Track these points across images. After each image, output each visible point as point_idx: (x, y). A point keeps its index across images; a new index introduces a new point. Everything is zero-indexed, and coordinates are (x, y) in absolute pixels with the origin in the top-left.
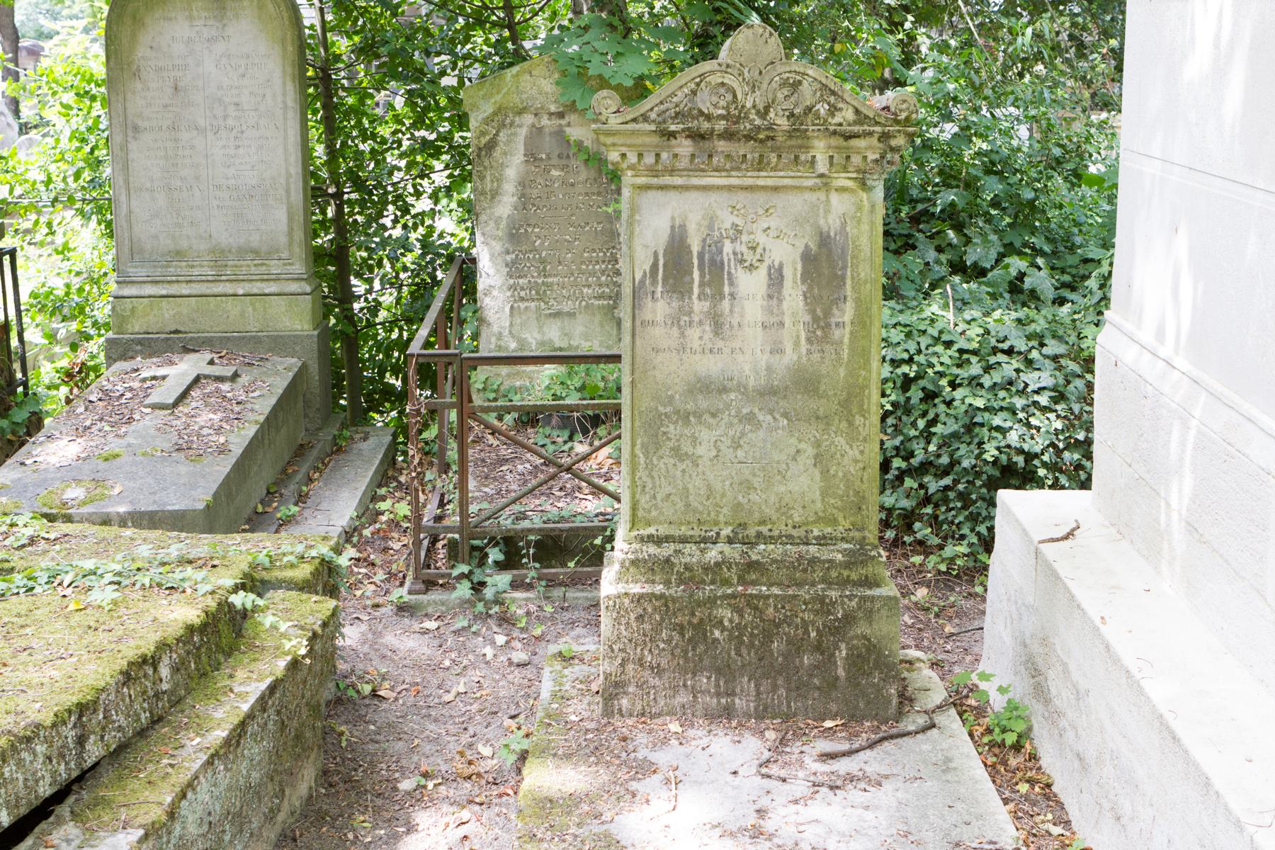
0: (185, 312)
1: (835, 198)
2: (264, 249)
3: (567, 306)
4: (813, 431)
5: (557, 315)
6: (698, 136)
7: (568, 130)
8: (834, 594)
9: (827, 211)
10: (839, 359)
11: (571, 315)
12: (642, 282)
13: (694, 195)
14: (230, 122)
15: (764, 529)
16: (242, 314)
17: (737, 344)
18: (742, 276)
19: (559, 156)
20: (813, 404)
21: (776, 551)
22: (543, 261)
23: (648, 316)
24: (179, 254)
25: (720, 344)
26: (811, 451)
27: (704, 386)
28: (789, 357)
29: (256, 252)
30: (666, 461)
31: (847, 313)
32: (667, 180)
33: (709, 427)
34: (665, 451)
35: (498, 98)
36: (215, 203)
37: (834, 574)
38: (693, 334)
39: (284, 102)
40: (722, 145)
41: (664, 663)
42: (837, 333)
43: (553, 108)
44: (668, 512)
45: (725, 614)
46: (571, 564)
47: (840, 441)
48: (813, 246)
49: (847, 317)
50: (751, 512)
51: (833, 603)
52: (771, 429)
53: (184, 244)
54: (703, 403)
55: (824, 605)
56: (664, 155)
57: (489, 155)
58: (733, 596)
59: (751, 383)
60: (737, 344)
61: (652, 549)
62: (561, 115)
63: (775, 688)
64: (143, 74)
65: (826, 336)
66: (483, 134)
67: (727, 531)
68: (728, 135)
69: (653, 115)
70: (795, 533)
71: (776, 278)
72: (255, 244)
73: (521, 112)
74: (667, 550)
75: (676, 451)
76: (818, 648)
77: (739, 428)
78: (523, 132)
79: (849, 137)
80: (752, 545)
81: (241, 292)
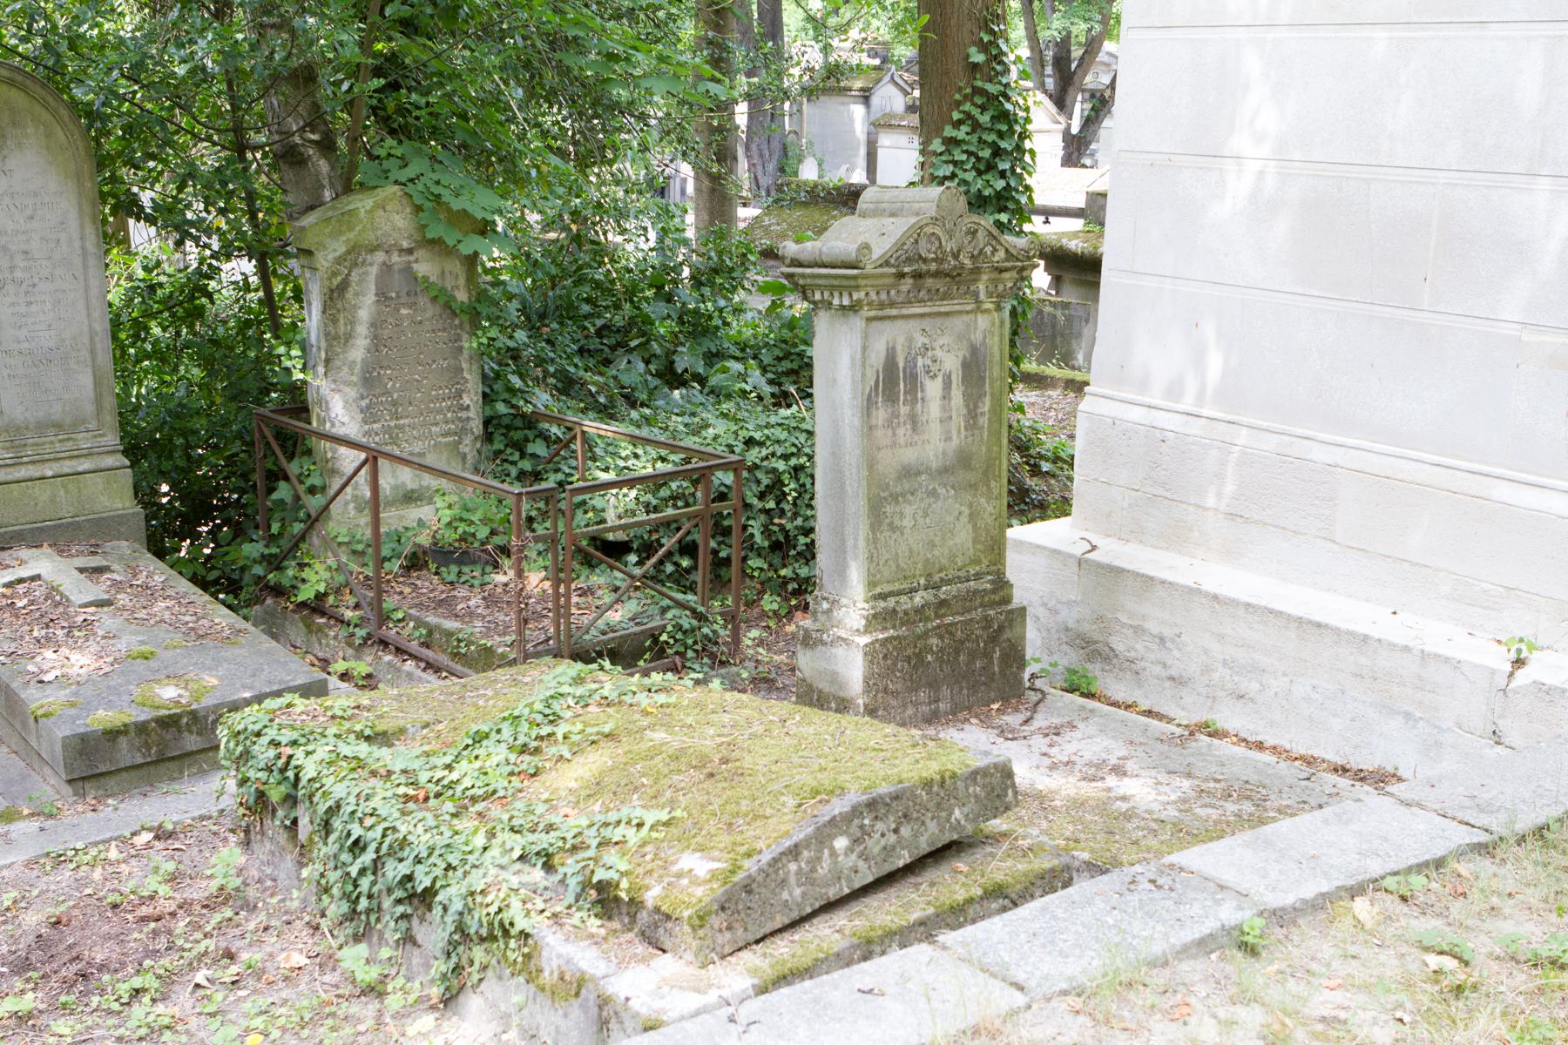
1: (980, 317)
4: (968, 496)
8: (992, 612)
13: (900, 322)
17: (926, 437)
23: (873, 422)
26: (967, 511)
28: (955, 441)
34: (884, 527)
38: (901, 431)
45: (934, 641)
52: (946, 499)
55: (987, 621)
58: (938, 627)
60: (926, 437)
61: (882, 604)
68: (937, 274)
79: (1001, 271)
80: (937, 587)
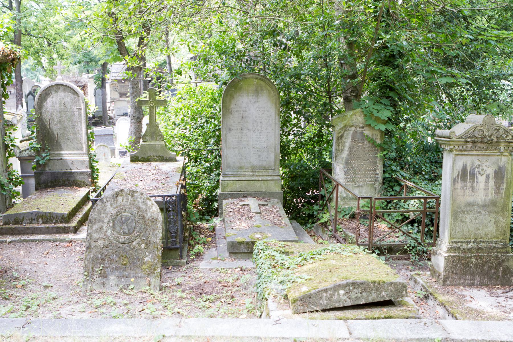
0: (243, 185)
1: (503, 158)
2: (267, 166)
3: (361, 184)
4: (494, 215)
5: (358, 186)
6: (474, 142)
7: (364, 132)
8: (500, 255)
9: (501, 161)
10: (502, 198)
11: (362, 186)
12: (455, 178)
13: (469, 157)
14: (259, 128)
15: (482, 240)
16: (261, 186)
17: (477, 194)
18: (480, 177)
19: (361, 140)
20: (495, 209)
21: (485, 245)
22: (355, 171)
23: (456, 187)
24: (241, 168)
25: (473, 194)
26: (494, 220)
27: (469, 204)
28: (490, 197)
29: (265, 167)
30: (458, 223)
31: (504, 186)
32: (464, 153)
33: (470, 215)
34: (459, 220)
35: (345, 122)
36: (253, 152)
37: (499, 250)
38: (467, 191)
39: (275, 122)
40: (479, 144)
41: (458, 272)
42: (501, 191)
43: (361, 125)
44: (458, 235)
45: (474, 260)
46: (397, 254)
47: (501, 218)
48: (497, 170)
49: (504, 187)
50: (478, 236)
51: (499, 257)
52: (484, 215)
53: (243, 165)
54: (468, 209)
55: (497, 258)
56: (464, 147)
57: (341, 139)
58: (476, 256)
59: (480, 203)
60: (477, 194)
61: (455, 245)
62: (363, 127)
63: (484, 278)
64: (233, 113)
65: (499, 192)
66: (340, 133)
67: (473, 240)
69: (463, 137)
70: (489, 240)
71: (488, 177)
72: (264, 165)
73: (351, 126)
74: (459, 245)
75: (461, 221)
76: (495, 268)
77: (477, 215)
78: (351, 132)
80: (479, 243)
81: (260, 179)
